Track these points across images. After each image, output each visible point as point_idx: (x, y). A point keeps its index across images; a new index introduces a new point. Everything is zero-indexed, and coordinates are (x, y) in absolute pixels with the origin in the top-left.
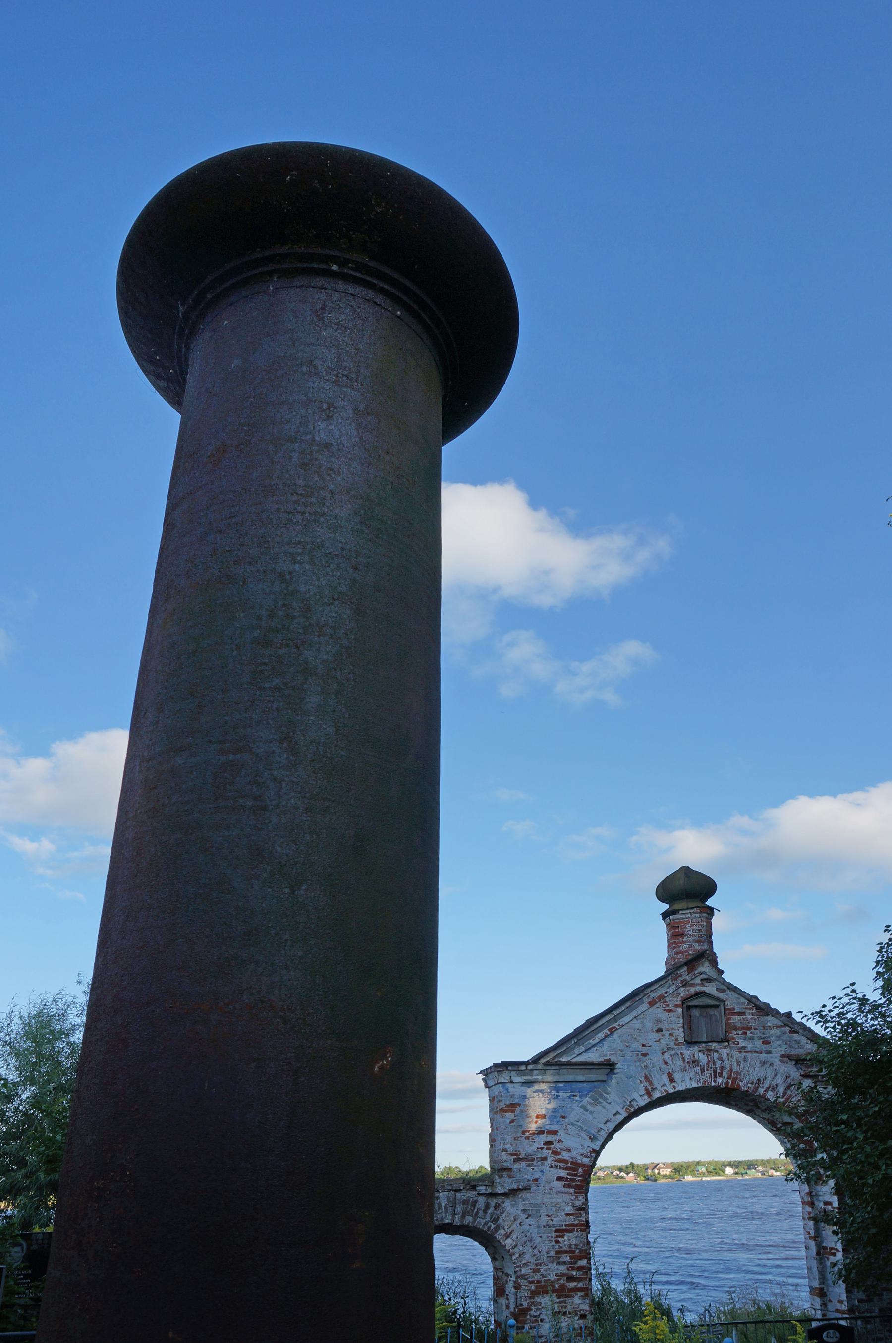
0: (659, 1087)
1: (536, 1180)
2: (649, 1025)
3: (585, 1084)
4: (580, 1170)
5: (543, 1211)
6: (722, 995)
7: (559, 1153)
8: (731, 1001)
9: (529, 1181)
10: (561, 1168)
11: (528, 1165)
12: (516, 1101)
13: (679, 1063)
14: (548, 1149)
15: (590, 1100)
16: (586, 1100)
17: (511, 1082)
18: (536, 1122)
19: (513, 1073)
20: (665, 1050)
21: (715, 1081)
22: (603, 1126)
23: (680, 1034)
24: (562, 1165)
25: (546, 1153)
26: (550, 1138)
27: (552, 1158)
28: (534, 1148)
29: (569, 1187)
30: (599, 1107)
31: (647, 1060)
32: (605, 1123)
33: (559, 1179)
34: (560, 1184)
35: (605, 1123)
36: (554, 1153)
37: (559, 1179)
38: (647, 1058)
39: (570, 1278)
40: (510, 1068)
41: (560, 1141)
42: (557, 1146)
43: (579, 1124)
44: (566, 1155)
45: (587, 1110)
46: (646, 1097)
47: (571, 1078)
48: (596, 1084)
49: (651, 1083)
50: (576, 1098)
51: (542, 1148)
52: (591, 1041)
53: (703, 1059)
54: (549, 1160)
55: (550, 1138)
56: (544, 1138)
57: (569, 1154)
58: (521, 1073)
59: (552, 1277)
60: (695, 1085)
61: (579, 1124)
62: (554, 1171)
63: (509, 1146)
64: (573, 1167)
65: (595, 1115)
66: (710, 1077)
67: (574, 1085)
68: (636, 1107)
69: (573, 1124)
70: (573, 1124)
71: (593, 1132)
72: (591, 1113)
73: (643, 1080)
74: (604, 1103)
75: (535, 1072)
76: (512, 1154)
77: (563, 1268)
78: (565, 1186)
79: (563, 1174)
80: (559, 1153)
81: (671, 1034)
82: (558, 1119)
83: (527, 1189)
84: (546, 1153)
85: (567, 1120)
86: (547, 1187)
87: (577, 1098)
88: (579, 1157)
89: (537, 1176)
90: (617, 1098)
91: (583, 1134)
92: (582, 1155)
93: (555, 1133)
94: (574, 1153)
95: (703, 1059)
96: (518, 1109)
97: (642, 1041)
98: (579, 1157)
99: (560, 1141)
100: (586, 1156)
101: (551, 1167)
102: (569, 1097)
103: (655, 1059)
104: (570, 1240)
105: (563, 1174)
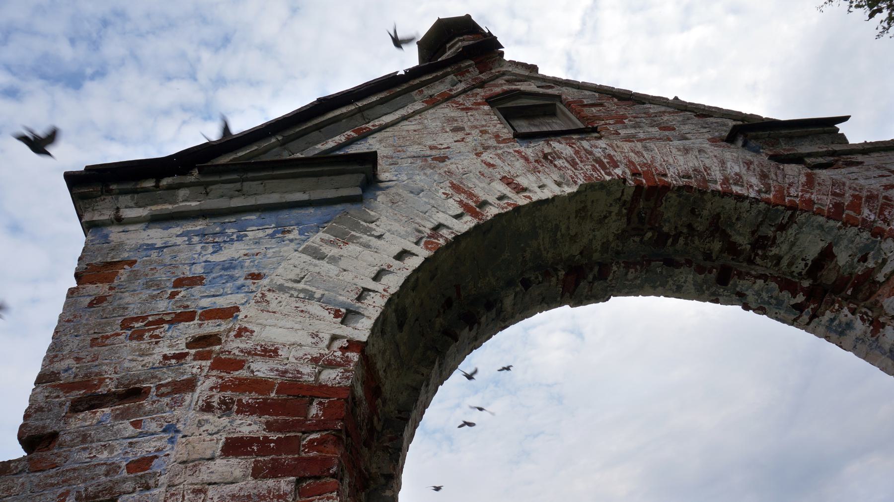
0: (492, 199)
1: (142, 464)
3: (311, 210)
4: (314, 410)
7: (238, 364)
9: (112, 469)
10: (245, 409)
11: (122, 416)
12: (125, 255)
13: (519, 164)
14: (199, 357)
15: (327, 236)
16: (316, 239)
17: (119, 221)
18: (173, 295)
19: (125, 200)
20: (480, 149)
21: (609, 174)
22: (372, 285)
24: (246, 399)
25: (192, 367)
27: (209, 383)
28: (157, 358)
29: (276, 471)
30: (352, 248)
31: (449, 165)
32: (377, 278)
33: (235, 447)
34: (237, 466)
35: (377, 278)
37: (235, 447)
38: (448, 162)
40: (114, 187)
41: (241, 332)
42: (234, 346)
43: (301, 286)
44: (262, 369)
45: (322, 257)
46: (467, 218)
48: (339, 207)
49: (471, 195)
50: (291, 236)
51: (180, 357)
52: (319, 146)
54: (203, 388)
55: (210, 327)
56: (192, 329)
57: (272, 364)
58: (143, 197)
60: (568, 190)
61: (301, 286)
62: (215, 421)
63: (70, 362)
64: (287, 399)
65: (343, 264)
66: (594, 169)
67: (284, 215)
68: (450, 237)
69: (282, 288)
70: (282, 288)
71: (347, 298)
72: (334, 260)
73: (449, 191)
74: (365, 238)
75: (183, 193)
76: (69, 387)
78: (257, 473)
79: (249, 427)
80: (238, 364)
81: (483, 132)
82: (241, 281)
84: (192, 367)
85: (265, 282)
86: (187, 481)
87: (295, 234)
88: (307, 370)
89: (147, 447)
90: (396, 226)
91: (315, 308)
92: (315, 360)
93: (229, 313)
94: (290, 358)
96: (124, 274)
97: (430, 143)
98: (307, 370)
99: (241, 332)
100: (331, 364)
101: (208, 408)
102: (272, 236)
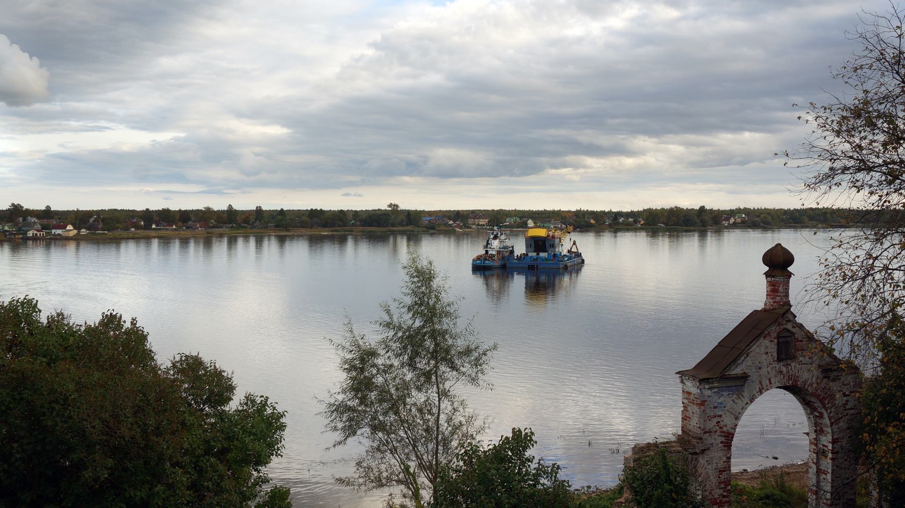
2: (763, 350)
5: (715, 461)
6: (794, 330)
8: (798, 334)
23: (775, 355)
26: (719, 419)
33: (722, 442)
36: (721, 428)
37: (722, 442)
39: (724, 496)
42: (722, 424)
44: (725, 429)
47: (729, 384)
53: (784, 370)
56: (716, 420)
58: (709, 383)
59: (716, 496)
77: (721, 491)
83: (708, 449)
93: (720, 416)
95: (784, 370)
103: (764, 371)
104: (724, 476)
105: (723, 439)
